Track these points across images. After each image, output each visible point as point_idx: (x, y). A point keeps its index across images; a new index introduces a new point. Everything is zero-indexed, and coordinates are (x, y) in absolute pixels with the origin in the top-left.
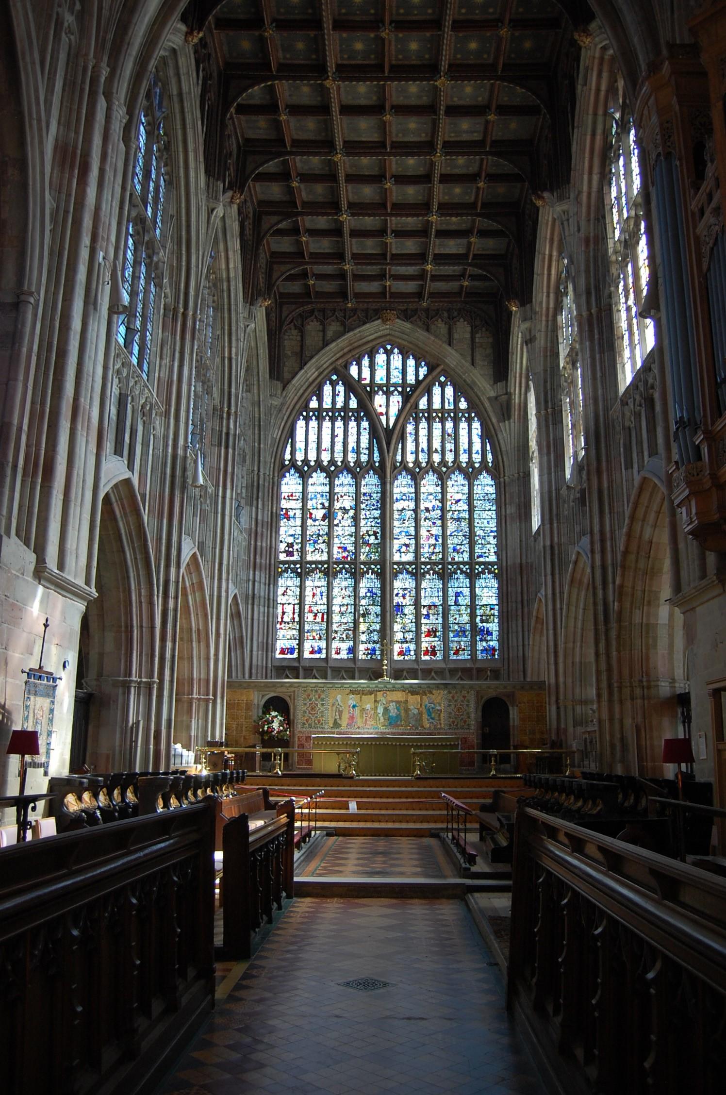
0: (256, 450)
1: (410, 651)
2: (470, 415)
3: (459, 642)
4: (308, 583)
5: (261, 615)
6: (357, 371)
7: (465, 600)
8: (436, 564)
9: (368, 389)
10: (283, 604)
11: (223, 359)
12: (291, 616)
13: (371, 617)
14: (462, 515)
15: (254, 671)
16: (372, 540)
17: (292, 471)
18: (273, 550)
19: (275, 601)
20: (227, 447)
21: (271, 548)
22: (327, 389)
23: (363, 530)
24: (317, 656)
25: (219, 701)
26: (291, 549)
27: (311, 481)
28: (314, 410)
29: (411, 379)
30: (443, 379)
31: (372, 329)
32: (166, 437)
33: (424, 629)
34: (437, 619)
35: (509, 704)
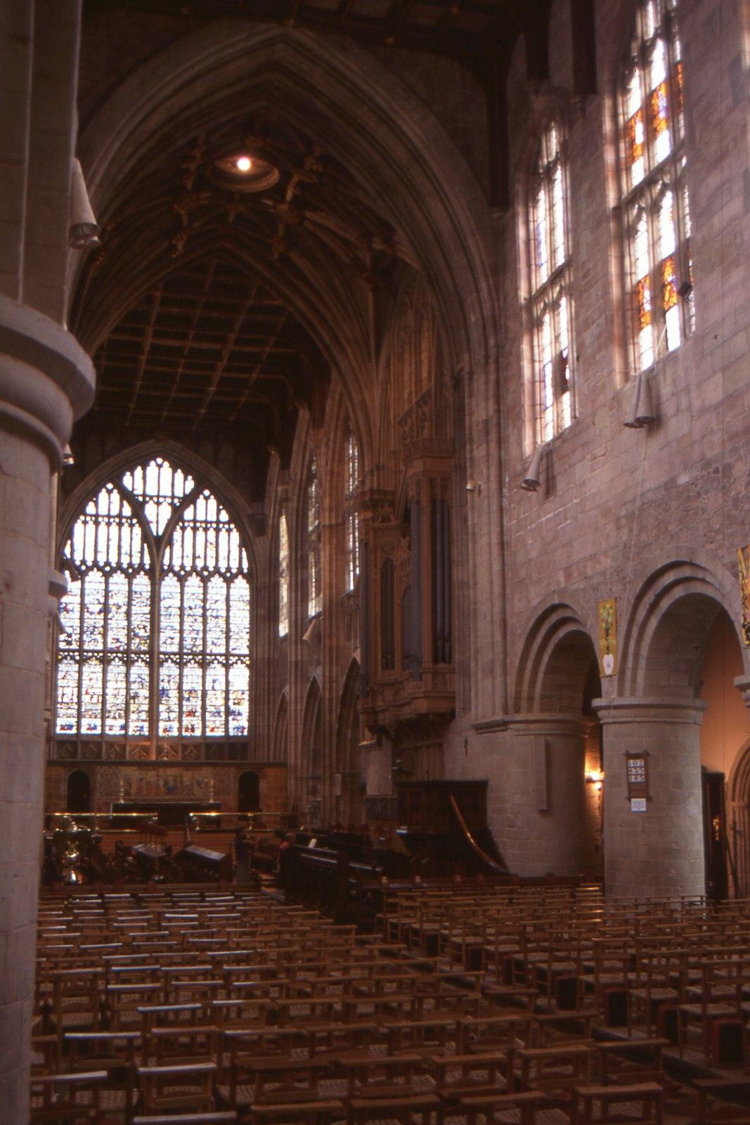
3: (214, 721)
7: (221, 686)
13: (140, 699)
14: (219, 614)
16: (142, 633)
22: (103, 495)
24: (94, 732)
29: (179, 493)
30: (207, 493)
33: (185, 709)
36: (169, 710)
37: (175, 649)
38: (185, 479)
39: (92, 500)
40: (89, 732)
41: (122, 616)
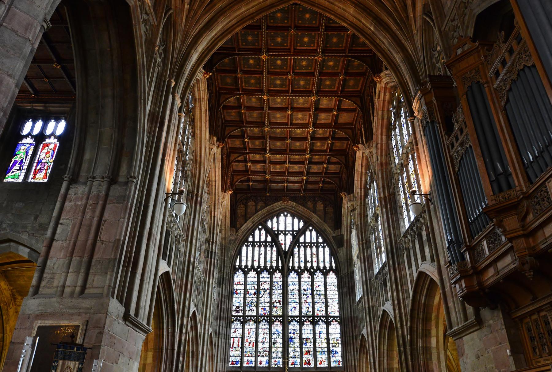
0: (223, 260)
2: (324, 245)
4: (247, 326)
5: (223, 343)
6: (271, 224)
7: (324, 336)
8: (310, 317)
9: (276, 232)
11: (211, 217)
12: (237, 344)
16: (278, 305)
17: (240, 271)
18: (229, 310)
19: (229, 336)
20: (211, 258)
21: (228, 309)
22: (257, 232)
23: (274, 300)
24: (250, 365)
26: (238, 309)
27: (248, 276)
28: (250, 242)
29: (296, 228)
30: (311, 228)
31: (278, 205)
32: (185, 252)
33: (304, 350)
36: (295, 352)
37: (297, 313)
38: (299, 222)
39: (251, 234)
40: (248, 365)
41: (267, 296)
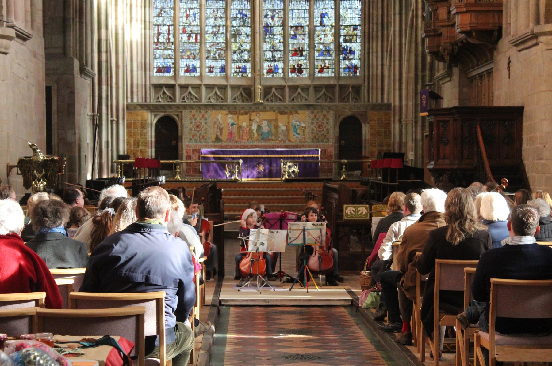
1: (278, 69)
3: (324, 61)
7: (330, 21)
10: (158, 26)
15: (135, 90)
25: (121, 121)
34: (303, 39)
35: (361, 121)
